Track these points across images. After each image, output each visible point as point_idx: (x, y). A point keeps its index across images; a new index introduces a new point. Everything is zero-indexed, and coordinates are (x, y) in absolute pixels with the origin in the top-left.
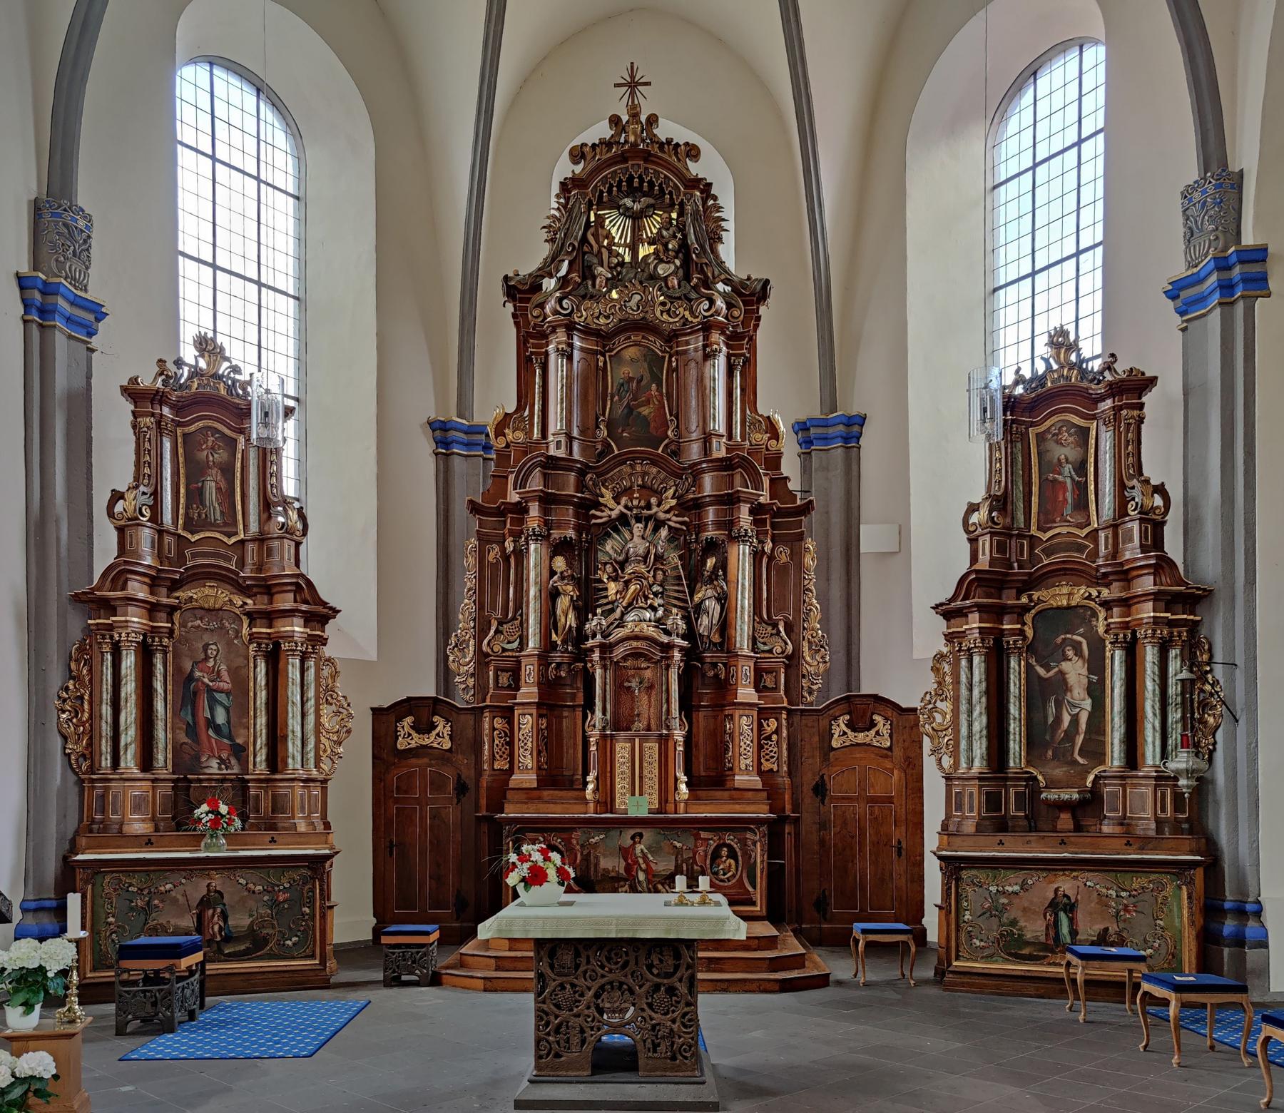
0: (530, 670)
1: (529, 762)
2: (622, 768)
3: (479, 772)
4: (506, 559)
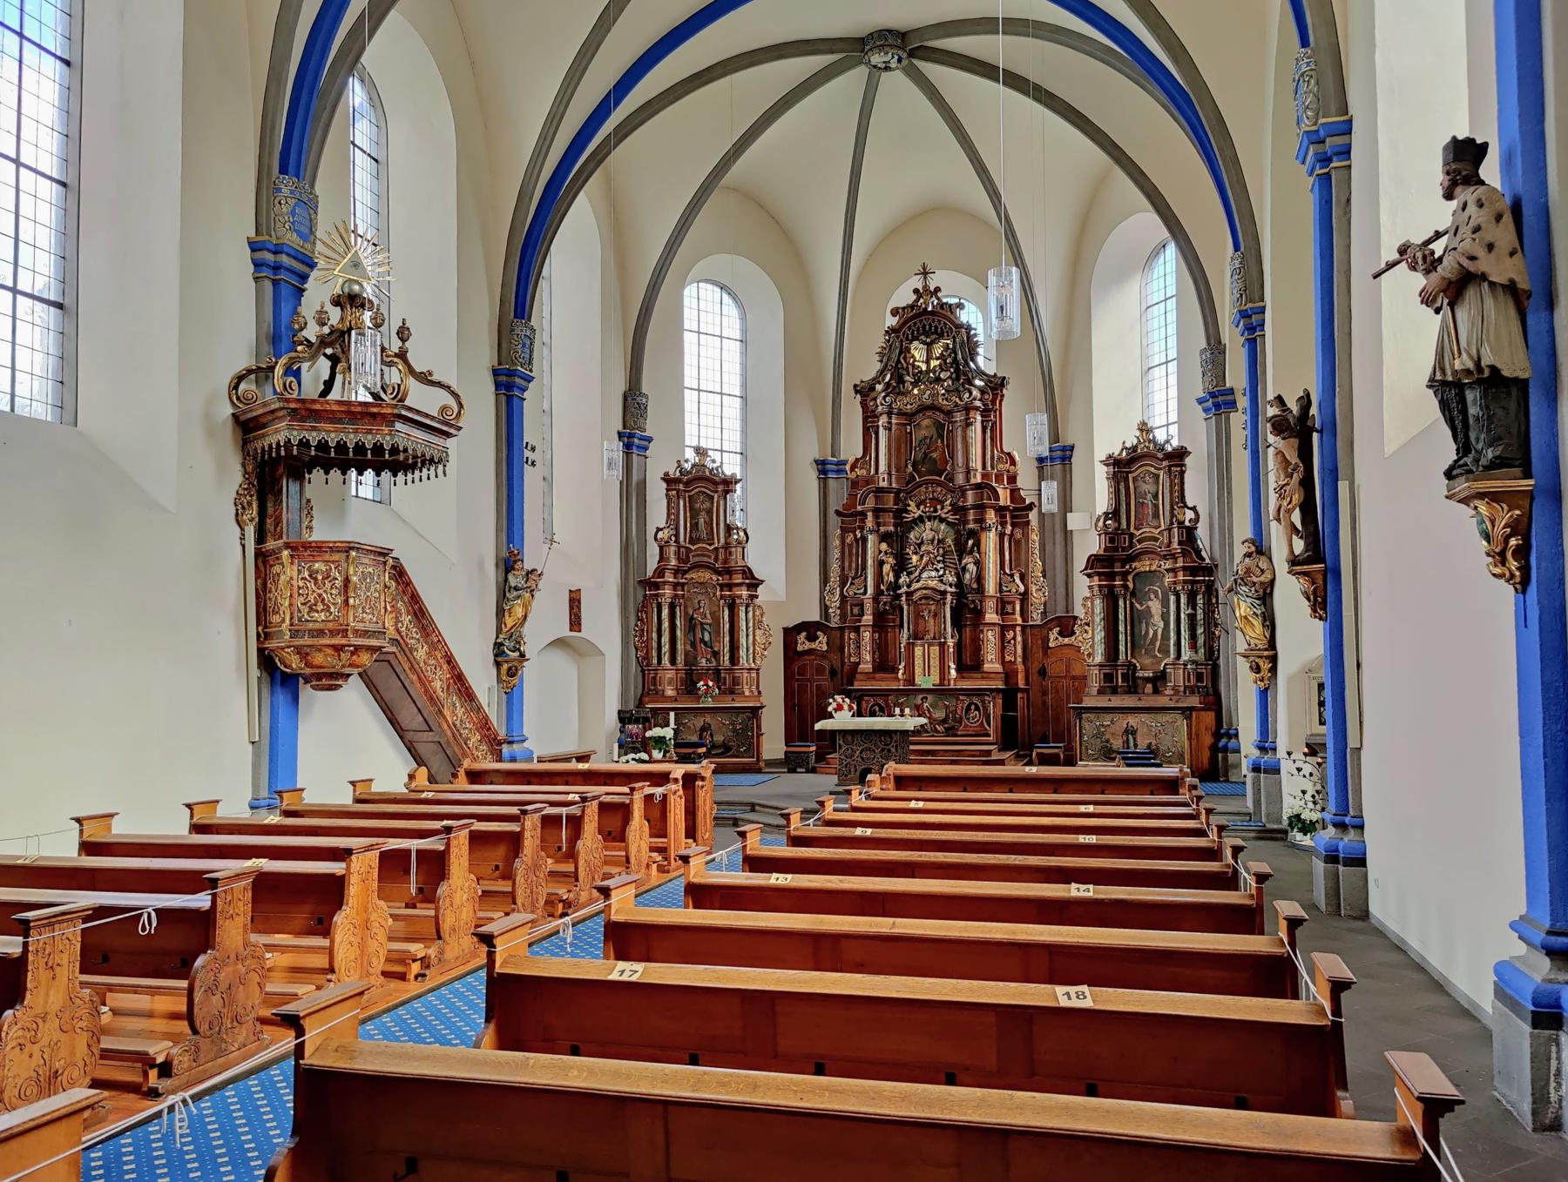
0: (868, 607)
1: (868, 658)
2: (918, 662)
3: (843, 663)
4: (857, 540)
